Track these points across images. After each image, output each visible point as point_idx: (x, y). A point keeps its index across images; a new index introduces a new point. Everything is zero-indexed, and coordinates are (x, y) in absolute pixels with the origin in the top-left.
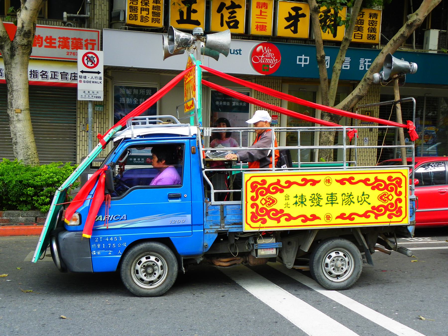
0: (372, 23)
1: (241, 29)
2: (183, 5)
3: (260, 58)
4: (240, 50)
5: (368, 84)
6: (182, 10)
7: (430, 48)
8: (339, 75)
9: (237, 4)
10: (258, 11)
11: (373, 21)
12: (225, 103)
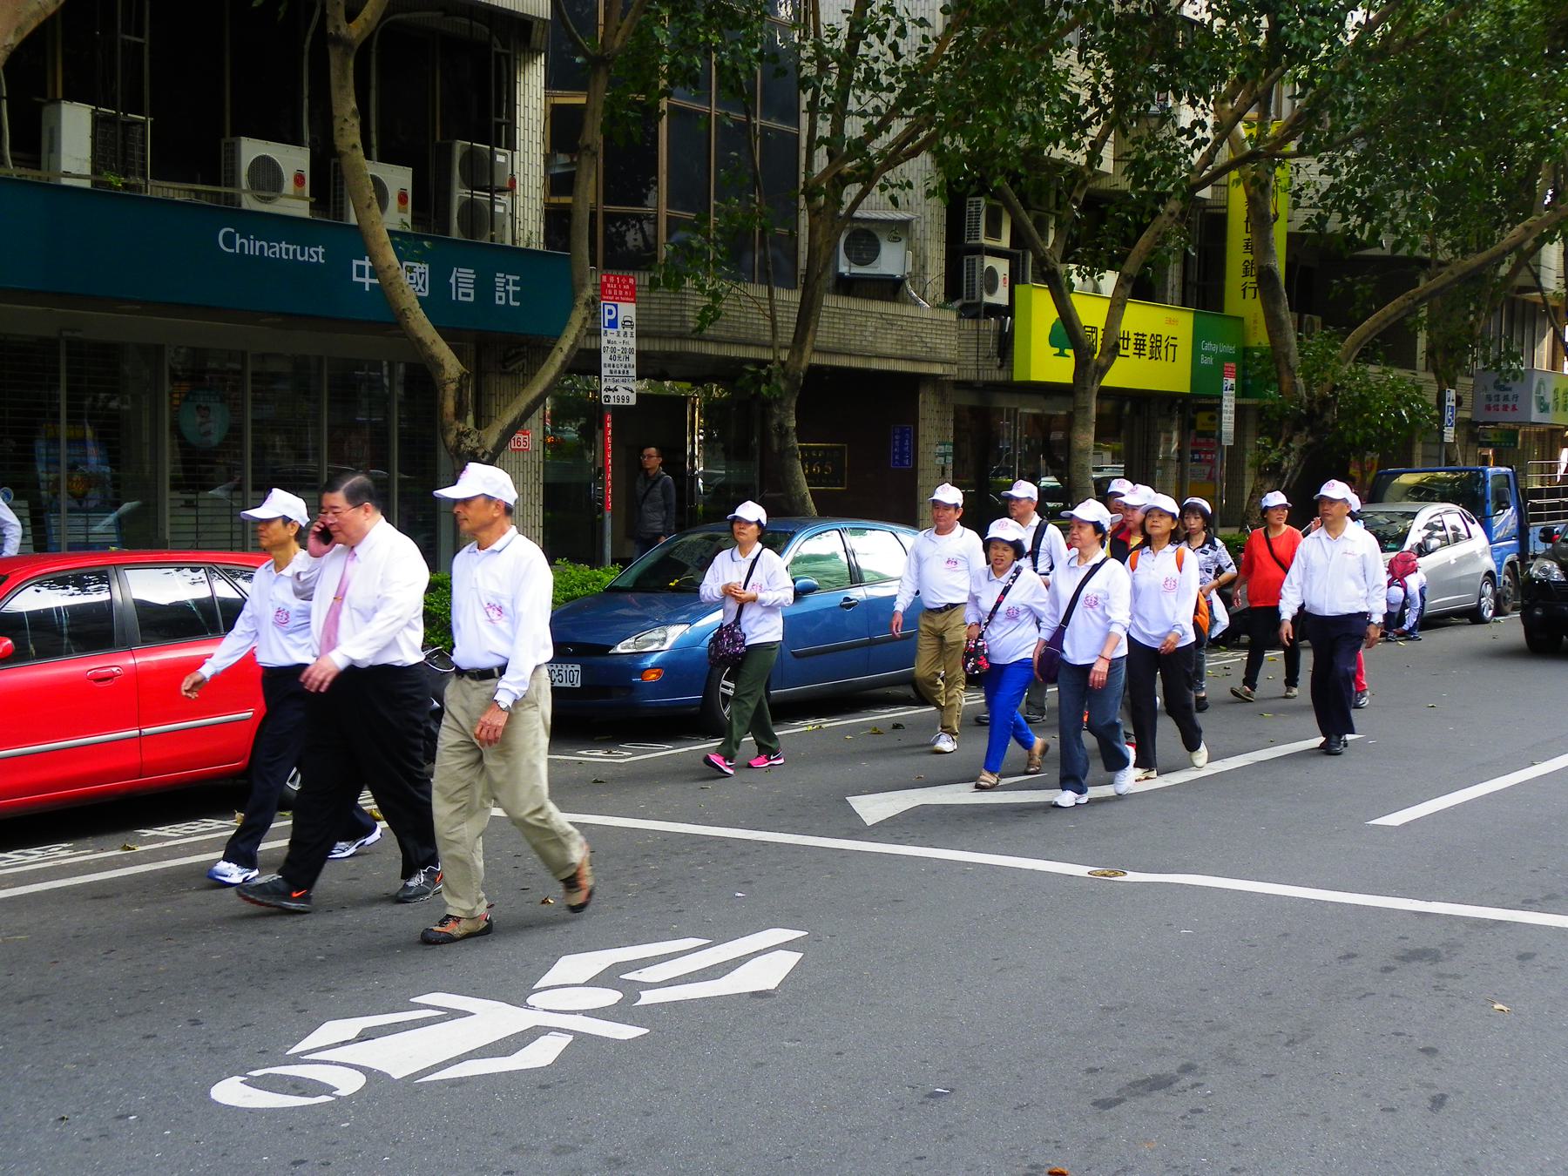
7: (64, 167)
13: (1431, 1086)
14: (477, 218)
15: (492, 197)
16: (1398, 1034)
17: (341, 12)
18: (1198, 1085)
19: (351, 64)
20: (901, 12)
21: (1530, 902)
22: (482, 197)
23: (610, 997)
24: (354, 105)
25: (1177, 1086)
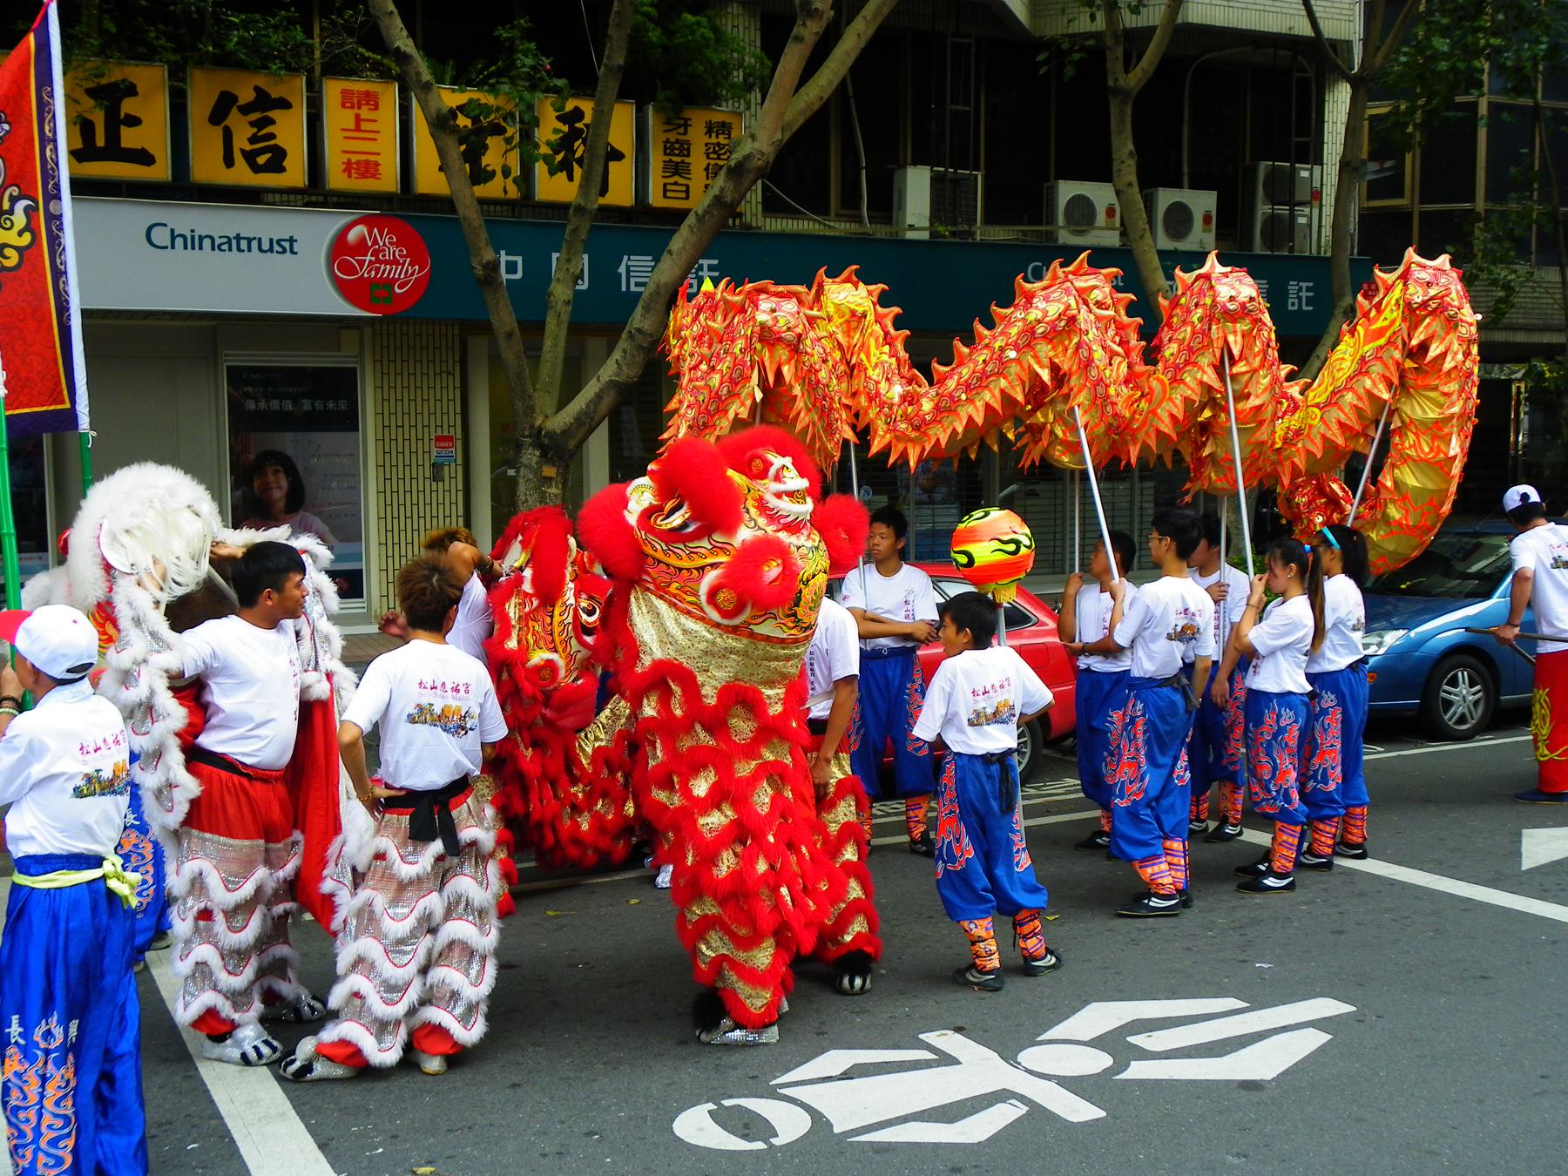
0: (714, 151)
1: (295, 173)
2: (89, 103)
3: (361, 263)
4: (292, 240)
5: (641, 347)
6: (86, 115)
7: (909, 221)
8: (565, 318)
9: (274, 95)
10: (347, 118)
11: (718, 144)
12: (275, 405)
14: (1281, 231)
15: (1292, 211)
17: (1120, 65)
19: (1129, 111)
22: (1283, 210)
23: (1100, 1061)
24: (1131, 147)
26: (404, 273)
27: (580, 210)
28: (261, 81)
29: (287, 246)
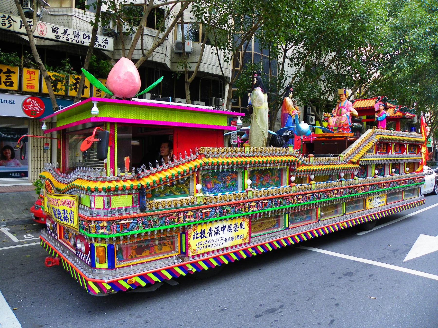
1: (16, 87)
3: (29, 107)
4: (14, 101)
10: (28, 76)
13: (332, 316)
16: (333, 299)
18: (281, 312)
20: (286, 74)
21: (378, 259)
25: (276, 312)
26: (39, 109)
27: (77, 98)
28: (9, 67)
29: (13, 102)
